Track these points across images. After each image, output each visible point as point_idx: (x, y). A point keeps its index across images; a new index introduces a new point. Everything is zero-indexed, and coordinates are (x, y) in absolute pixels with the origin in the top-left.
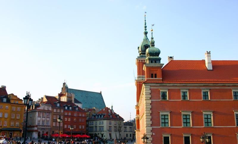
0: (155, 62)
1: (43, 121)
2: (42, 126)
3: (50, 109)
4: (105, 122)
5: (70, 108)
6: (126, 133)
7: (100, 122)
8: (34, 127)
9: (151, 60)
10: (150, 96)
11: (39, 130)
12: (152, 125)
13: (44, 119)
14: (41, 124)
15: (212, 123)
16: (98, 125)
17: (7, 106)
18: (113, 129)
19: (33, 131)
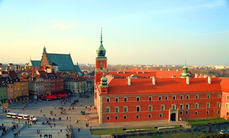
0: (105, 85)
1: (39, 89)
2: (39, 91)
3: (43, 80)
4: (75, 83)
5: (54, 78)
6: (88, 88)
7: (72, 83)
8: (34, 92)
9: (103, 84)
10: (102, 101)
11: (37, 94)
12: (102, 113)
13: (39, 87)
14: (38, 90)
15: (127, 111)
16: (71, 84)
17: (18, 84)
18: (80, 87)
19: (34, 95)
